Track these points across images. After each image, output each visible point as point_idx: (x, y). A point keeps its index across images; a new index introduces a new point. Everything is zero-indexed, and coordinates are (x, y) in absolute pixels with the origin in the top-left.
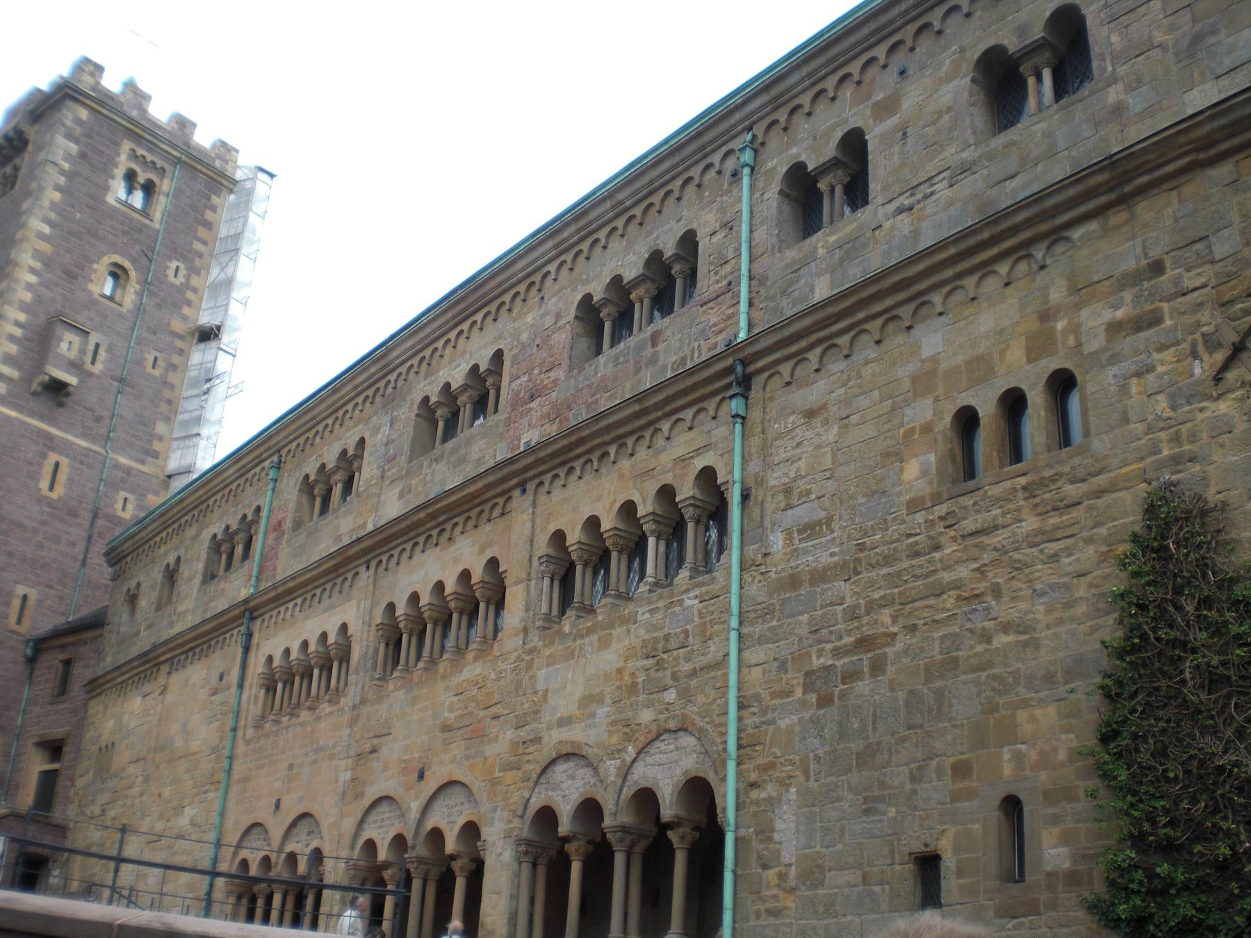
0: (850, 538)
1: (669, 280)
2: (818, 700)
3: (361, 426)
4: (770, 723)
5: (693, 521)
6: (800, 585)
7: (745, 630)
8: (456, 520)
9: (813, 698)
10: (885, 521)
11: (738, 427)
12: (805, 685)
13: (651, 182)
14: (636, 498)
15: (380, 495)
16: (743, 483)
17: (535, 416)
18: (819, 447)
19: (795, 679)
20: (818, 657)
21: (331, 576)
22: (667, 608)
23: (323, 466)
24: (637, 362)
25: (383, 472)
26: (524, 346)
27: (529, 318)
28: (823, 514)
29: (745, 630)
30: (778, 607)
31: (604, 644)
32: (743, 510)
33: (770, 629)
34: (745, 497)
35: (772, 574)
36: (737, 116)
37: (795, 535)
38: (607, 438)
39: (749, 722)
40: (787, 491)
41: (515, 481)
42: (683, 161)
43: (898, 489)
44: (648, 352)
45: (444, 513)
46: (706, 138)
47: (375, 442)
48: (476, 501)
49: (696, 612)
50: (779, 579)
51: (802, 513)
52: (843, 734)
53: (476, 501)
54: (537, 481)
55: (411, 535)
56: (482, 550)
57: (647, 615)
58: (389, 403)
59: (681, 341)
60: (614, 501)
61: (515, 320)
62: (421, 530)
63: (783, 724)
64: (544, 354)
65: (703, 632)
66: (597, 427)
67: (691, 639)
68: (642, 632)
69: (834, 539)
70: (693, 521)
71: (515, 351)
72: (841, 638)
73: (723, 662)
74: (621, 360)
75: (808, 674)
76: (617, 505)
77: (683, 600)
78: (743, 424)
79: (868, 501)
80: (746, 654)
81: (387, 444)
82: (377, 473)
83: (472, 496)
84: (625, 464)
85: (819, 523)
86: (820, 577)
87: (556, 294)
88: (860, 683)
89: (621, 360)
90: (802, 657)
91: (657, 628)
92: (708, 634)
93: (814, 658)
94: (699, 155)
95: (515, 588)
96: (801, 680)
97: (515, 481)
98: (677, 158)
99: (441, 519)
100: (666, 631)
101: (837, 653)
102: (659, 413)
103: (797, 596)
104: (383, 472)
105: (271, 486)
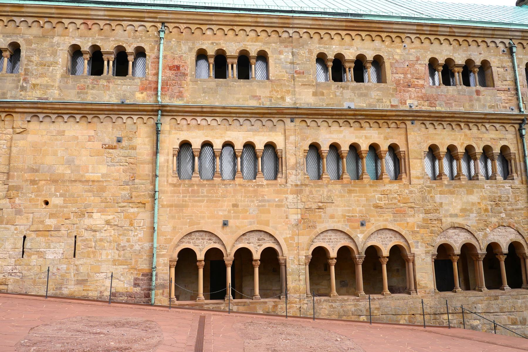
1: (476, 73)
13: (470, 33)
36: (510, 33)
42: (484, 34)
46: (496, 32)
48: (385, 118)
55: (334, 117)
57: (489, 187)
68: (488, 192)
83: (385, 116)
94: (491, 36)
98: (482, 32)
99: (360, 117)
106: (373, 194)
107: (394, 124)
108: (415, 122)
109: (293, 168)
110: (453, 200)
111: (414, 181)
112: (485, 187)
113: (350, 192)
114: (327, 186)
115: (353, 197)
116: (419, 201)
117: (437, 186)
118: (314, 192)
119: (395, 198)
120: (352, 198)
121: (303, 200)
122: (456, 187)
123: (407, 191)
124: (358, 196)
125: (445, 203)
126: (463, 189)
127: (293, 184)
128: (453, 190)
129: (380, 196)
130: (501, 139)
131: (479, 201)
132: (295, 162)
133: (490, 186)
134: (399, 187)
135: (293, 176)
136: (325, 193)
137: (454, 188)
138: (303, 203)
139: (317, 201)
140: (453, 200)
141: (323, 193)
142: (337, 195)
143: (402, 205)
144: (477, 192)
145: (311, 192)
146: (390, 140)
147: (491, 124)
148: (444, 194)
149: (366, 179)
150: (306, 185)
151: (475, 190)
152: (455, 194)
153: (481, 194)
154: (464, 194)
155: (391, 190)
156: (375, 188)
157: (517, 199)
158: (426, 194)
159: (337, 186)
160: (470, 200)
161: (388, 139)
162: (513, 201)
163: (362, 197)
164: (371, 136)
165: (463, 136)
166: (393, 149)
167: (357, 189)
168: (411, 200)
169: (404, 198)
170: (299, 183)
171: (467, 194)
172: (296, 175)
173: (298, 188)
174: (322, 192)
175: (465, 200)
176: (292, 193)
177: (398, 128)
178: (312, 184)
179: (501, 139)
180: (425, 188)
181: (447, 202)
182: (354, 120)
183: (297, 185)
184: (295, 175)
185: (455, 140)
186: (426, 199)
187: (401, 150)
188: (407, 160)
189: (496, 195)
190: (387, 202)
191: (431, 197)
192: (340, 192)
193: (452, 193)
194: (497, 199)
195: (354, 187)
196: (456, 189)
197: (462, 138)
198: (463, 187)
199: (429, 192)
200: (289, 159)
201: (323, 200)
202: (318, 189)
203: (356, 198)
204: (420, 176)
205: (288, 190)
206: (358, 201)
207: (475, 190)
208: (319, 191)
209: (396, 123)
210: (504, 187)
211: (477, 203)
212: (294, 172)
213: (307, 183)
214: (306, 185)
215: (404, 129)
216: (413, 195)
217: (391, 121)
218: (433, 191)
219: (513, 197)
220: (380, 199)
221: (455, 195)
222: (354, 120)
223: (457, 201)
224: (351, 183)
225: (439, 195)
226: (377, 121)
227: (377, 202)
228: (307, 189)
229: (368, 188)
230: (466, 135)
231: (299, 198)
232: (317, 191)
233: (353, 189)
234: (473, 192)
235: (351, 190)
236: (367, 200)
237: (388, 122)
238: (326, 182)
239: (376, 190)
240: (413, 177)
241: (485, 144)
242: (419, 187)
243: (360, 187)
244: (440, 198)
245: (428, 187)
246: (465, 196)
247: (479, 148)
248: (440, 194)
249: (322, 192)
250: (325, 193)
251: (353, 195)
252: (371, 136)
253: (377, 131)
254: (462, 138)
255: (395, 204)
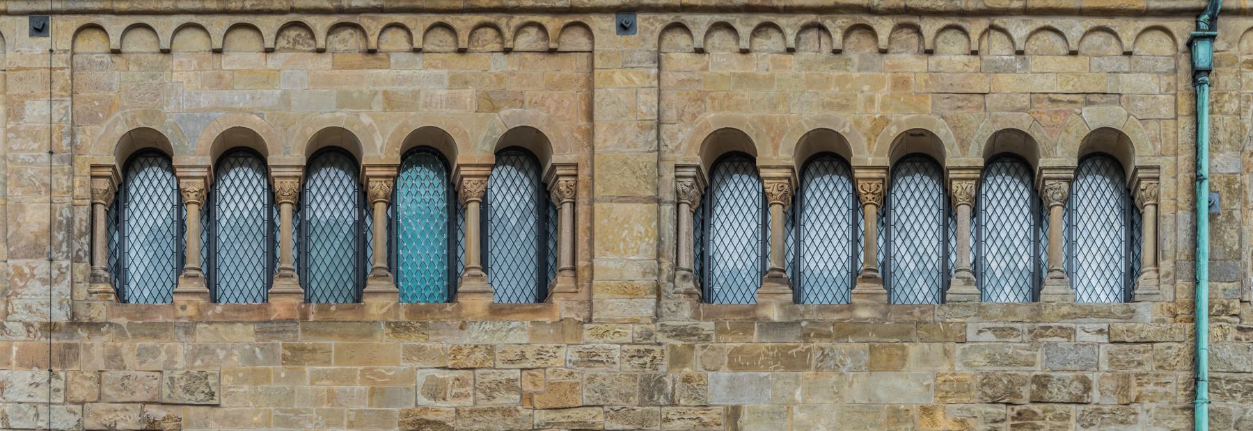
49: (1103, 355)
56: (489, 103)
57: (989, 336)
65: (1124, 389)
67: (1095, 395)
68: (979, 360)
92: (1133, 394)
95: (620, 209)
100: (1038, 370)
106: (406, 366)
107: (533, 31)
108: (641, 19)
109: (34, 250)
110: (798, 396)
111: (610, 306)
112: (971, 335)
113: (296, 355)
114: (189, 329)
115: (310, 381)
116: (627, 397)
117: (721, 331)
118: (130, 359)
119: (510, 385)
120: (306, 386)
121: (79, 393)
122: (819, 335)
123: (568, 353)
124: (331, 376)
125: (753, 412)
126: (852, 344)
127: (36, 319)
128: (802, 346)
129: (439, 374)
130: (1088, 98)
131: (932, 402)
132: (47, 221)
133: (994, 330)
134: (533, 333)
135: (37, 287)
136: (181, 362)
137: (806, 337)
138: (78, 408)
139: (139, 396)
140: (798, 396)
141: (171, 362)
142: (234, 373)
143: (540, 417)
144: (924, 359)
145: (114, 358)
146: (505, 112)
147: (1040, 22)
148: (756, 368)
149: (380, 300)
150: (94, 326)
151: (914, 350)
152: (807, 367)
153: (945, 368)
154: (856, 369)
155: (490, 350)
156: (414, 340)
157: (1133, 394)
158: (663, 369)
159: (239, 328)
160: (882, 394)
161: (495, 109)
162: (1109, 403)
163: (350, 379)
164: (415, 95)
165: (886, 90)
166: (522, 151)
167: (332, 343)
168: (585, 396)
169: (552, 386)
170: (61, 317)
171: (871, 368)
172: (50, 281)
173: (58, 340)
174: (163, 357)
175: (855, 392)
176: (27, 362)
177: (552, 52)
178: (123, 321)
179: (1088, 98)
180: (660, 337)
181: (764, 406)
182: (334, 19)
183: (50, 328)
184: (44, 281)
185: (842, 107)
186: (661, 391)
187: (555, 159)
188: (582, 209)
189: (1024, 372)
190: (469, 402)
191: (687, 380)
192: (251, 358)
193: (792, 362)
194: (1026, 392)
195: (319, 334)
196: (816, 344)
197: (878, 97)
198: (854, 333)
199: (678, 359)
200: (20, 207)
201: (166, 391)
202: (149, 343)
203: (324, 386)
204: (640, 282)
205: (9, 350)
206: (332, 396)
207: (914, 350)
208: (154, 352)
209: (541, 27)
210: (1069, 333)
211: (915, 411)
212: (42, 266)
213: (102, 318)
214: (94, 326)
215: (583, 60)
216: (600, 370)
217: (517, 20)
218: (698, 352)
219: (1110, 384)
220: (436, 391)
221: (810, 374)
222: (334, 19)
223: (814, 400)
224: (304, 317)
225: (725, 374)
226: (448, 19)
227: (423, 401)
228: (98, 346)
229: (383, 338)
230: (901, 83)
231: (56, 384)
232: (142, 354)
233: (309, 342)
234: (904, 358)
235: (303, 349)
236: (373, 392)
237: (502, 21)
238: (191, 310)
239: (420, 349)
240: (606, 289)
241: (999, 127)
242: (630, 332)
243: (343, 336)
244: (732, 387)
245: (679, 333)
246: (863, 376)
247: (964, 144)
248: (734, 366)
249: (163, 357)
250: (181, 362)
251: (307, 369)
252: (415, 95)
253: (444, 72)
254: (878, 97)
255: (507, 412)
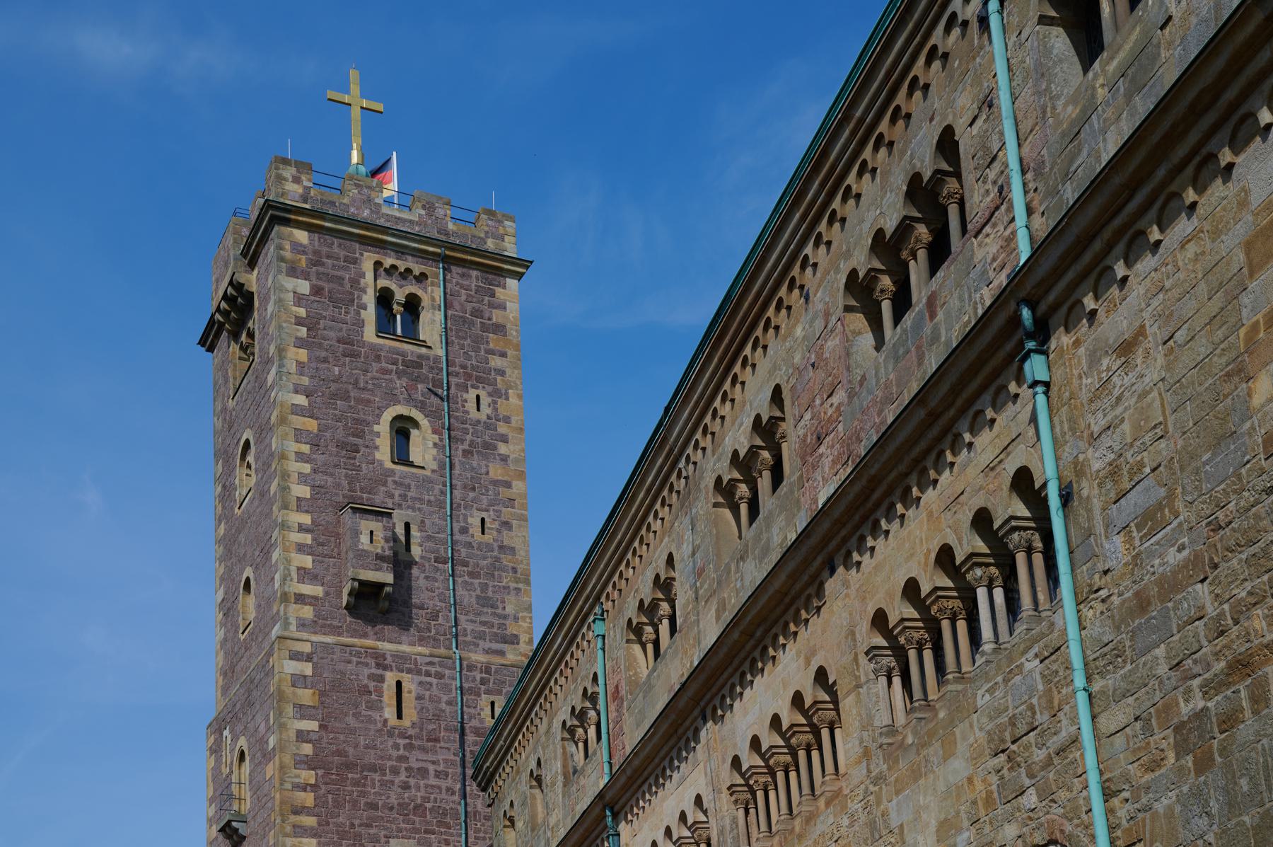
0: (1200, 519)
2: (1195, 763)
3: (666, 539)
4: (1147, 809)
5: (1010, 551)
6: (1149, 603)
7: (1096, 687)
8: (774, 631)
9: (1189, 761)
10: (1239, 477)
11: (1041, 399)
12: (1176, 745)
14: (951, 540)
15: (698, 621)
16: (1060, 479)
17: (827, 462)
18: (1145, 394)
19: (1163, 739)
20: (1187, 700)
21: (671, 743)
22: (1006, 681)
23: (642, 601)
24: (919, 348)
25: (696, 592)
26: (799, 371)
27: (799, 331)
28: (1162, 492)
29: (1096, 687)
30: (1128, 644)
31: (948, 755)
32: (1066, 517)
33: (1124, 677)
34: (1066, 498)
35: (1114, 598)
37: (1135, 534)
38: (902, 468)
39: (1122, 813)
40: (1114, 472)
41: (819, 560)
43: (1248, 425)
44: (928, 329)
45: (759, 625)
47: (683, 554)
50: (1124, 602)
51: (1136, 501)
52: (1232, 805)
53: (787, 600)
54: (843, 551)
58: (686, 498)
59: (961, 299)
60: (929, 551)
61: (785, 339)
62: (742, 655)
63: (1159, 807)
64: (821, 374)
66: (886, 456)
69: (1180, 524)
70: (1010, 551)
71: (793, 381)
72: (1208, 667)
73: (1075, 741)
74: (901, 352)
75: (1178, 729)
76: (933, 555)
77: (1022, 664)
78: (1046, 393)
79: (1214, 455)
80: (1102, 720)
81: (693, 554)
82: (691, 593)
84: (930, 496)
85: (1160, 506)
86: (1171, 586)
87: (819, 286)
88: (1241, 726)
89: (901, 352)
90: (1168, 709)
91: (1000, 712)
93: (1182, 704)
96: (1171, 740)
97: (819, 560)
101: (1209, 689)
102: (952, 412)
103: (1148, 621)
104: (696, 592)
105: (600, 644)
